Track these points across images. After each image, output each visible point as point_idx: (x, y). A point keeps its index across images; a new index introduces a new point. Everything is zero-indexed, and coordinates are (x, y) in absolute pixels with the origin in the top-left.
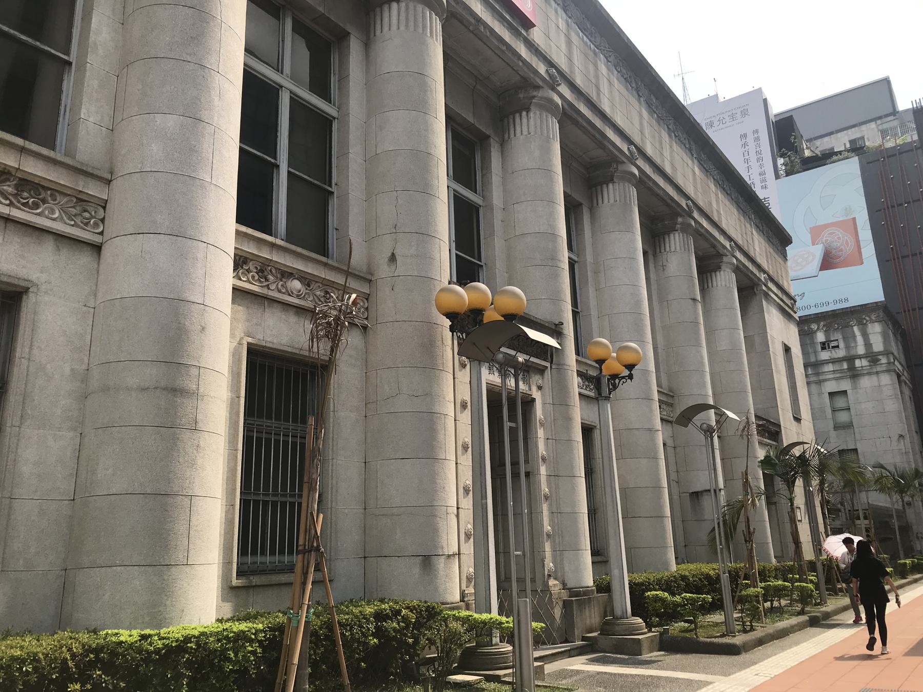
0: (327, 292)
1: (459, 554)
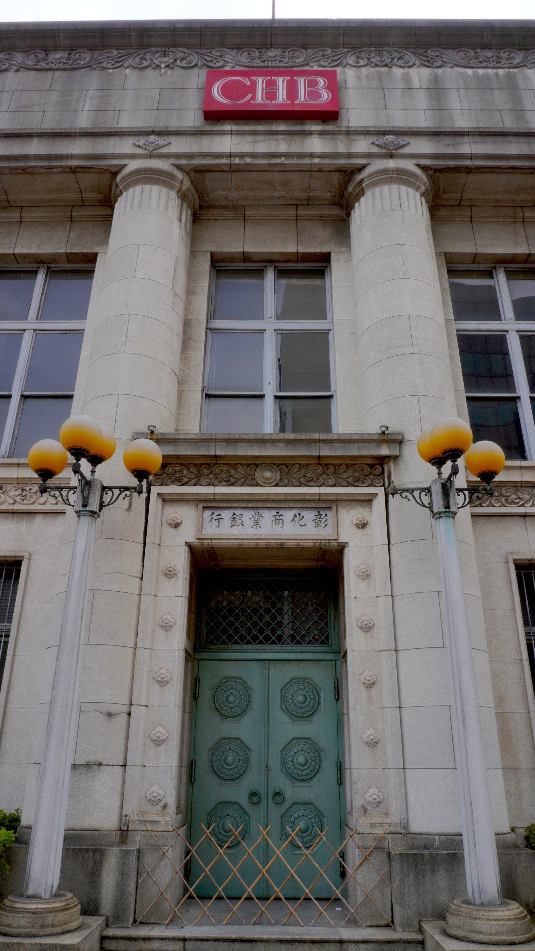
0: (23, 490)
1: (125, 765)
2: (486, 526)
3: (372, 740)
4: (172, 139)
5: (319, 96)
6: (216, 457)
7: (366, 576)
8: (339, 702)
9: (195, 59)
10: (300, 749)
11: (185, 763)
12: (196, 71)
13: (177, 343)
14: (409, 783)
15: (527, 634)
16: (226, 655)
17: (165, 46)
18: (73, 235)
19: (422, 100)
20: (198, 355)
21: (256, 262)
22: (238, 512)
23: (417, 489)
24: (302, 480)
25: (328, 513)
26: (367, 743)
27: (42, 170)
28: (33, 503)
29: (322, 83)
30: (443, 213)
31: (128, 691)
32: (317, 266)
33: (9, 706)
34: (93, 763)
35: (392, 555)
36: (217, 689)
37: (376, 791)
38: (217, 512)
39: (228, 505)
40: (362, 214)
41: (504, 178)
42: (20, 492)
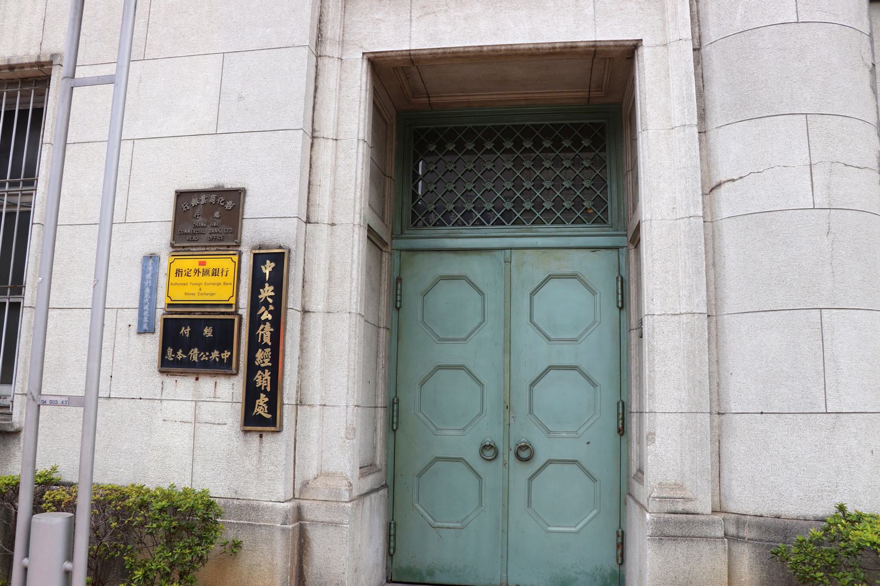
8: (624, 313)
11: (380, 401)
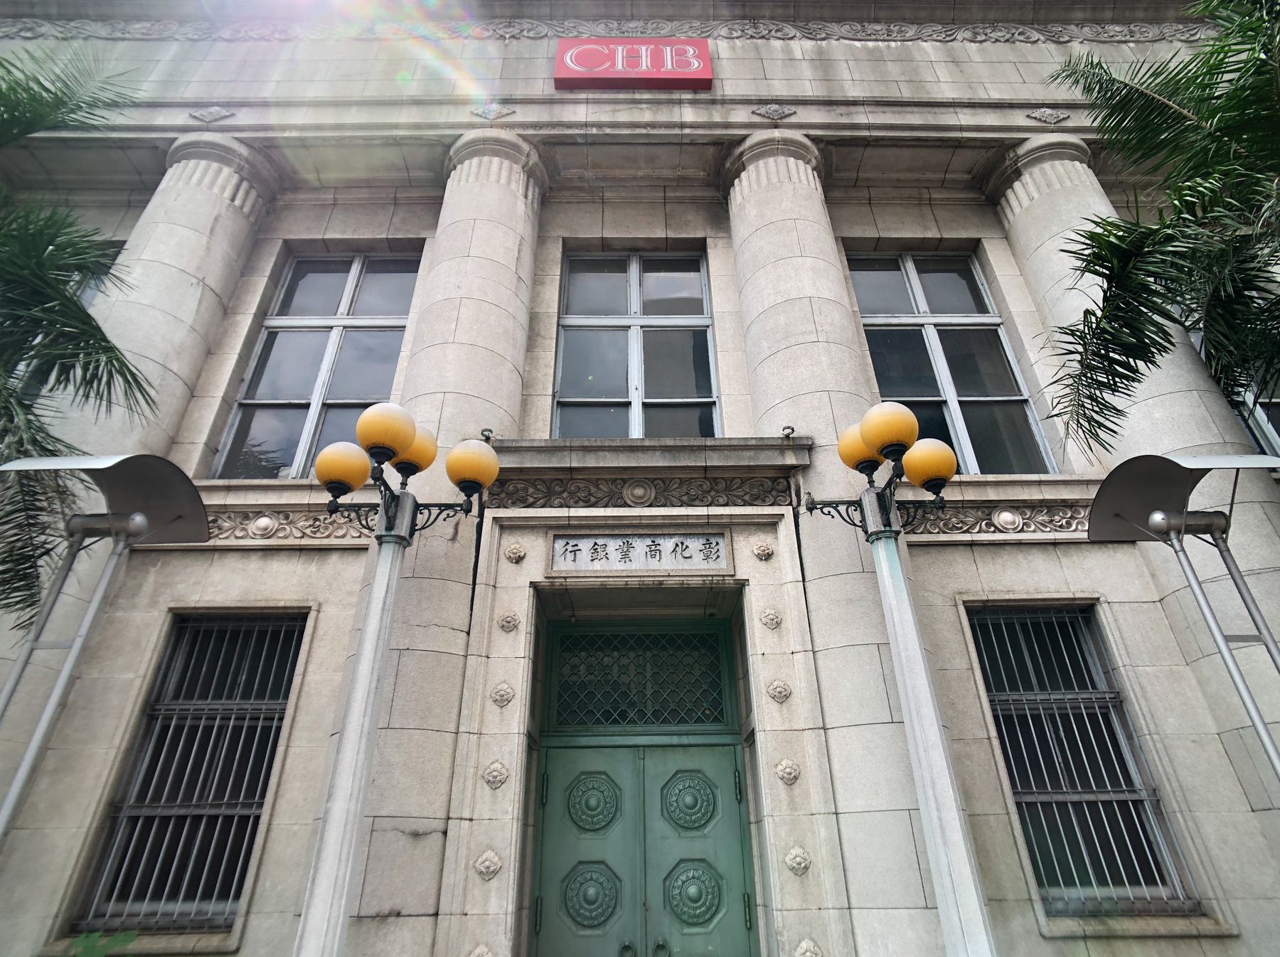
0: (316, 520)
1: (436, 914)
2: (924, 559)
3: (799, 864)
4: (518, 108)
5: (689, 64)
6: (571, 469)
7: (775, 624)
8: (743, 805)
9: (544, 30)
10: (691, 875)
12: (545, 41)
13: (521, 337)
14: (857, 931)
15: (991, 701)
16: (584, 741)
17: (511, 17)
18: (396, 220)
19: (807, 71)
20: (547, 356)
21: (616, 250)
22: (600, 541)
23: (843, 503)
24: (685, 498)
25: (720, 540)
26: (792, 869)
27: (362, 142)
28: (328, 537)
29: (692, 52)
30: (837, 194)
31: (444, 798)
32: (690, 256)
33: (275, 822)
34: (387, 912)
35: (810, 595)
36: (571, 788)
37: (812, 944)
38: (572, 542)
39: (588, 532)
40: (744, 191)
41: (907, 152)
42: (311, 522)
